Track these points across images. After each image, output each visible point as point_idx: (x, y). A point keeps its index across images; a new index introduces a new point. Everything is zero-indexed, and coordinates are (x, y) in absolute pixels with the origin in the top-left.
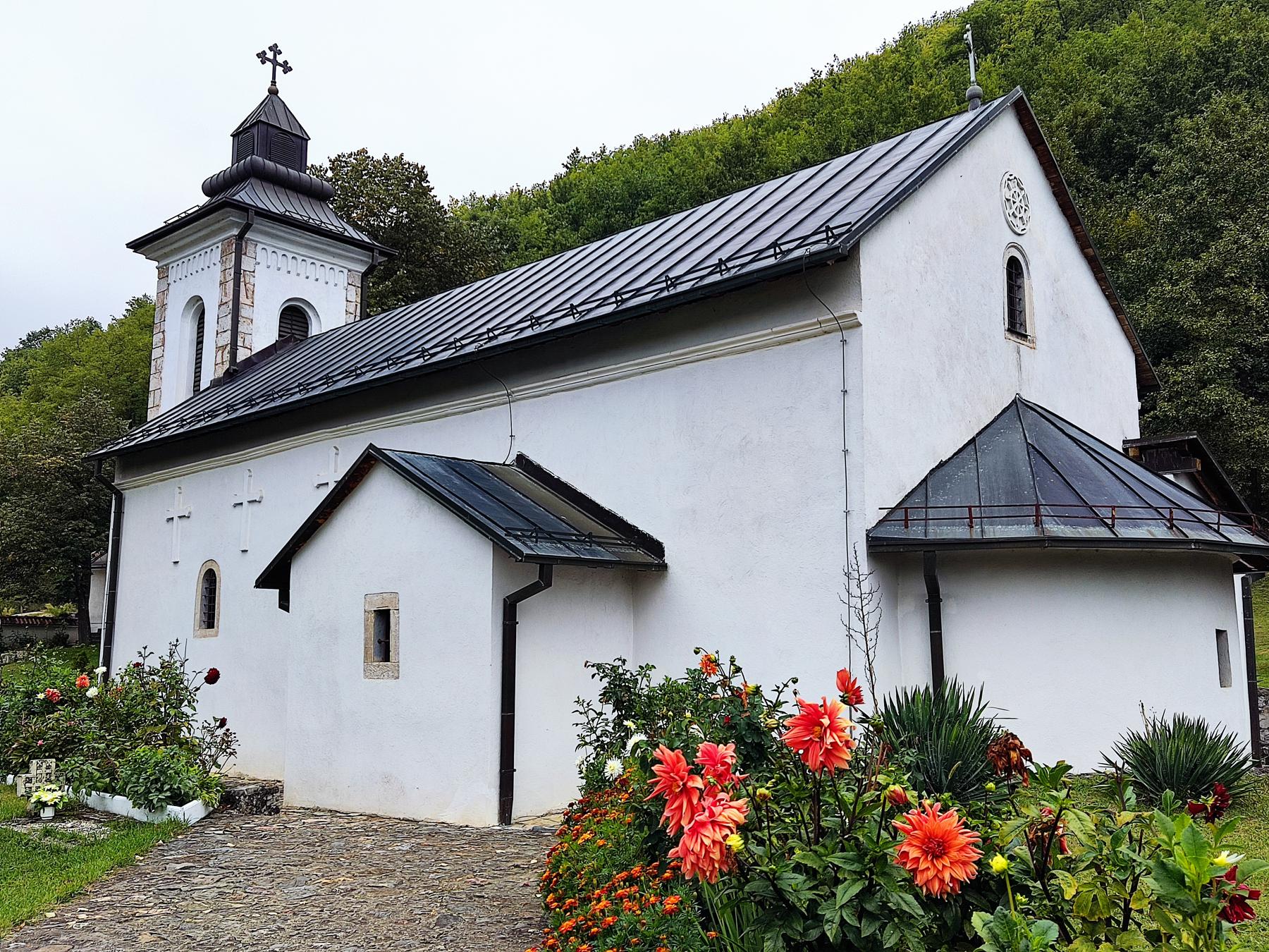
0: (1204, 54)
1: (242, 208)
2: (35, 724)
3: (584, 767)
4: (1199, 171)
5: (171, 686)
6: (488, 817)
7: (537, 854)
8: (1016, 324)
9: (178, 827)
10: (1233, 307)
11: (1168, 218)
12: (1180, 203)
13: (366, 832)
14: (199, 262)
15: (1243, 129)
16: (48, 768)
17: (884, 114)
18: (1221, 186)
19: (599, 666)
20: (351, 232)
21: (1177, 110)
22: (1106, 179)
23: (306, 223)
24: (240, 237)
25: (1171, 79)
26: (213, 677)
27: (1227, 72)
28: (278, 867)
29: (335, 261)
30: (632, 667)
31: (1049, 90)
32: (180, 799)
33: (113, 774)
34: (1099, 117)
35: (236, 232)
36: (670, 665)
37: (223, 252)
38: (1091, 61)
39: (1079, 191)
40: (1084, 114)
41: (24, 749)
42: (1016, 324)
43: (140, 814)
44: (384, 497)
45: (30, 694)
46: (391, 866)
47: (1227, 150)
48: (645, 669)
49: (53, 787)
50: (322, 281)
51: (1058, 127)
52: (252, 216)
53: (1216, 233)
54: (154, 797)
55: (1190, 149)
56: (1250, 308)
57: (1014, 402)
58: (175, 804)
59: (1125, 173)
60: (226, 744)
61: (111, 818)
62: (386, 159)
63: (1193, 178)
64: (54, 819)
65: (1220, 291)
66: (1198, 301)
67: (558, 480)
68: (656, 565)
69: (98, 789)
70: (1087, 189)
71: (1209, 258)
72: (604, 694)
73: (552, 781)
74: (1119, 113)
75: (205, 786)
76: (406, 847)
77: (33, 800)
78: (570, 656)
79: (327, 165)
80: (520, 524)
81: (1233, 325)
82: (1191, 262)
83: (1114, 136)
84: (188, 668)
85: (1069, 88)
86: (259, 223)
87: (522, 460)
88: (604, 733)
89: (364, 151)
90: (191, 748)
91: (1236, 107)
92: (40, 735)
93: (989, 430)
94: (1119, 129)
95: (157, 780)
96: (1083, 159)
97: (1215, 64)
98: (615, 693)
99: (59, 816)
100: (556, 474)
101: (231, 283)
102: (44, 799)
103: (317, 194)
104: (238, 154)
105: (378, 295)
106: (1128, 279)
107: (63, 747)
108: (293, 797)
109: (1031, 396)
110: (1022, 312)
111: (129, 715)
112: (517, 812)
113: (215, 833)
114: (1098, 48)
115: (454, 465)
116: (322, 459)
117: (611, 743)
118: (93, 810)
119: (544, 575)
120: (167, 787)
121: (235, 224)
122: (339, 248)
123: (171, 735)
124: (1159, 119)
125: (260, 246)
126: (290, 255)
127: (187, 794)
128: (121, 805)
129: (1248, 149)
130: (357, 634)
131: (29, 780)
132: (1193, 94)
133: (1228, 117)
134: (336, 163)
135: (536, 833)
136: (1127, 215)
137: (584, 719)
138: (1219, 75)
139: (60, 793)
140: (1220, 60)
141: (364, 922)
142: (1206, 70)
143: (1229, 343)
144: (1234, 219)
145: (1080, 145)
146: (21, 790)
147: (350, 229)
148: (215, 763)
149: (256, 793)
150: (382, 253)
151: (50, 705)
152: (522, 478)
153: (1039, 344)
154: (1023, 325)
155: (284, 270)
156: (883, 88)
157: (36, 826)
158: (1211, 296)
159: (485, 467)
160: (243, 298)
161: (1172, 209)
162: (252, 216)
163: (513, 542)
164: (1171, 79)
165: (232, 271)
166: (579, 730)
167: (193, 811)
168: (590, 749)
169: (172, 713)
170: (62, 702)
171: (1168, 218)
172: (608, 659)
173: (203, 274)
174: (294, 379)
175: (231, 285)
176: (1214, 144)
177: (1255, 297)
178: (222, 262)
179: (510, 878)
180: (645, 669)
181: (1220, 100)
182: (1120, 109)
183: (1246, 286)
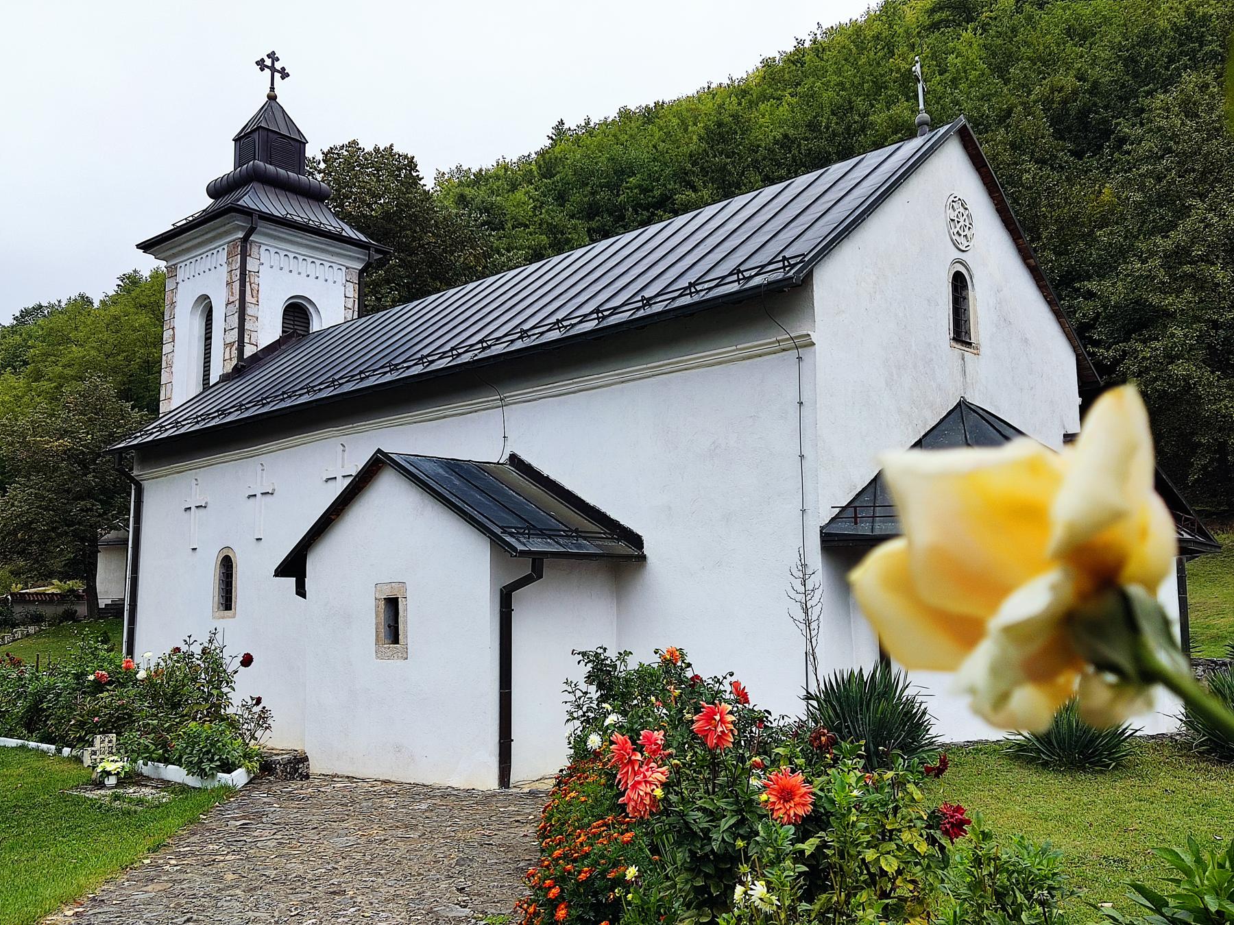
0: (1178, 29)
1: (247, 212)
2: (89, 703)
3: (572, 739)
4: (1169, 150)
5: (214, 669)
6: (490, 782)
7: (534, 811)
8: (961, 333)
9: (228, 790)
10: (1201, 285)
11: (1138, 197)
12: (1149, 182)
13: (388, 794)
14: (206, 262)
15: (1212, 109)
16: (110, 742)
17: (866, 85)
18: (1189, 165)
19: (584, 654)
20: (349, 232)
21: (1151, 86)
22: (1079, 155)
23: (307, 225)
24: (245, 240)
25: (1145, 55)
26: (247, 661)
27: (1201, 46)
28: (320, 822)
29: (334, 259)
30: (612, 654)
31: (1027, 64)
32: (228, 768)
33: (165, 745)
34: (1075, 92)
35: (241, 235)
36: (644, 656)
37: (229, 254)
38: (1070, 32)
39: (1053, 168)
40: (1061, 90)
41: (81, 725)
42: (961, 333)
43: (193, 781)
44: (391, 499)
45: (79, 676)
46: (414, 822)
47: (1197, 130)
48: (624, 655)
49: (116, 758)
50: (321, 279)
51: (1035, 102)
52: (256, 220)
53: (1184, 212)
54: (206, 766)
55: (1160, 129)
56: (1217, 285)
57: (959, 404)
58: (224, 772)
59: (1101, 147)
60: (263, 720)
61: (166, 785)
62: (377, 150)
63: (1162, 157)
64: (117, 786)
65: (1188, 268)
66: (1166, 279)
67: (547, 477)
68: (636, 557)
69: (153, 760)
70: (1060, 166)
71: (1178, 236)
72: (588, 677)
73: (544, 753)
74: (1095, 88)
75: (247, 756)
76: (424, 807)
77: (99, 770)
78: (563, 638)
79: (320, 157)
80: (514, 522)
81: (1201, 301)
82: (1159, 240)
83: (1090, 111)
84: (226, 654)
85: (1047, 62)
86: (263, 226)
87: (514, 459)
88: (589, 709)
89: (355, 142)
90: (232, 723)
91: (1206, 86)
92: (95, 713)
93: (935, 432)
94: (1095, 104)
95: (208, 752)
96: (1059, 135)
97: (1190, 38)
98: (597, 676)
99: (121, 783)
100: (545, 473)
101: (237, 284)
102: (108, 769)
103: (314, 196)
104: (240, 159)
105: (373, 295)
106: (1100, 256)
107: (118, 722)
108: (316, 766)
109: (976, 399)
110: (967, 321)
111: (175, 694)
112: (515, 777)
113: (260, 796)
114: (1076, 20)
115: (453, 466)
116: (335, 456)
117: (595, 718)
118: (149, 778)
119: (537, 567)
120: (217, 758)
121: (239, 228)
122: (337, 247)
123: (215, 713)
124: (1134, 94)
125: (263, 248)
126: (291, 255)
127: (233, 763)
128: (175, 773)
129: (1217, 130)
130: (369, 620)
131: (94, 753)
132: (1167, 69)
133: (1197, 97)
134: (329, 156)
135: (533, 794)
136: (1100, 192)
137: (571, 698)
138: (1193, 50)
139: (121, 764)
140: (1195, 34)
141: (399, 863)
142: (1181, 45)
143: (1197, 319)
144: (1202, 196)
145: (1055, 121)
146: (87, 761)
147: (347, 228)
148: (253, 737)
149: (289, 762)
150: (377, 251)
151: (99, 686)
152: (514, 475)
153: (983, 350)
154: (968, 333)
155: (286, 270)
156: (863, 60)
157: (103, 792)
158: (1179, 272)
159: (482, 467)
160: (248, 298)
161: (1142, 188)
162: (256, 220)
163: (508, 539)
164: (1145, 55)
165: (238, 272)
166: (568, 707)
167: (239, 777)
168: (577, 723)
169: (215, 692)
170: (110, 683)
171: (1138, 197)
172: (591, 647)
173: (206, 275)
174: (297, 377)
175: (237, 285)
176: (1183, 124)
177: (1220, 274)
178: (229, 264)
179: (512, 830)
180: (624, 655)
181: (1190, 79)
182: (1096, 84)
183: (1213, 264)
